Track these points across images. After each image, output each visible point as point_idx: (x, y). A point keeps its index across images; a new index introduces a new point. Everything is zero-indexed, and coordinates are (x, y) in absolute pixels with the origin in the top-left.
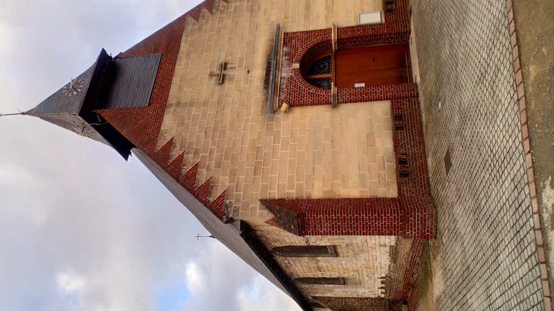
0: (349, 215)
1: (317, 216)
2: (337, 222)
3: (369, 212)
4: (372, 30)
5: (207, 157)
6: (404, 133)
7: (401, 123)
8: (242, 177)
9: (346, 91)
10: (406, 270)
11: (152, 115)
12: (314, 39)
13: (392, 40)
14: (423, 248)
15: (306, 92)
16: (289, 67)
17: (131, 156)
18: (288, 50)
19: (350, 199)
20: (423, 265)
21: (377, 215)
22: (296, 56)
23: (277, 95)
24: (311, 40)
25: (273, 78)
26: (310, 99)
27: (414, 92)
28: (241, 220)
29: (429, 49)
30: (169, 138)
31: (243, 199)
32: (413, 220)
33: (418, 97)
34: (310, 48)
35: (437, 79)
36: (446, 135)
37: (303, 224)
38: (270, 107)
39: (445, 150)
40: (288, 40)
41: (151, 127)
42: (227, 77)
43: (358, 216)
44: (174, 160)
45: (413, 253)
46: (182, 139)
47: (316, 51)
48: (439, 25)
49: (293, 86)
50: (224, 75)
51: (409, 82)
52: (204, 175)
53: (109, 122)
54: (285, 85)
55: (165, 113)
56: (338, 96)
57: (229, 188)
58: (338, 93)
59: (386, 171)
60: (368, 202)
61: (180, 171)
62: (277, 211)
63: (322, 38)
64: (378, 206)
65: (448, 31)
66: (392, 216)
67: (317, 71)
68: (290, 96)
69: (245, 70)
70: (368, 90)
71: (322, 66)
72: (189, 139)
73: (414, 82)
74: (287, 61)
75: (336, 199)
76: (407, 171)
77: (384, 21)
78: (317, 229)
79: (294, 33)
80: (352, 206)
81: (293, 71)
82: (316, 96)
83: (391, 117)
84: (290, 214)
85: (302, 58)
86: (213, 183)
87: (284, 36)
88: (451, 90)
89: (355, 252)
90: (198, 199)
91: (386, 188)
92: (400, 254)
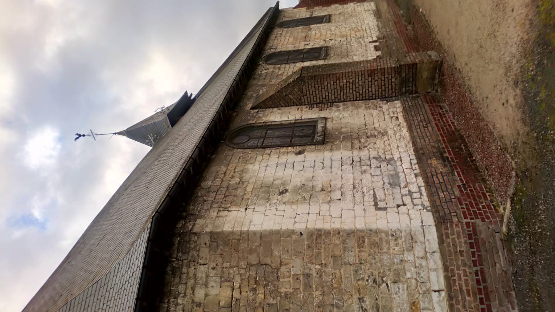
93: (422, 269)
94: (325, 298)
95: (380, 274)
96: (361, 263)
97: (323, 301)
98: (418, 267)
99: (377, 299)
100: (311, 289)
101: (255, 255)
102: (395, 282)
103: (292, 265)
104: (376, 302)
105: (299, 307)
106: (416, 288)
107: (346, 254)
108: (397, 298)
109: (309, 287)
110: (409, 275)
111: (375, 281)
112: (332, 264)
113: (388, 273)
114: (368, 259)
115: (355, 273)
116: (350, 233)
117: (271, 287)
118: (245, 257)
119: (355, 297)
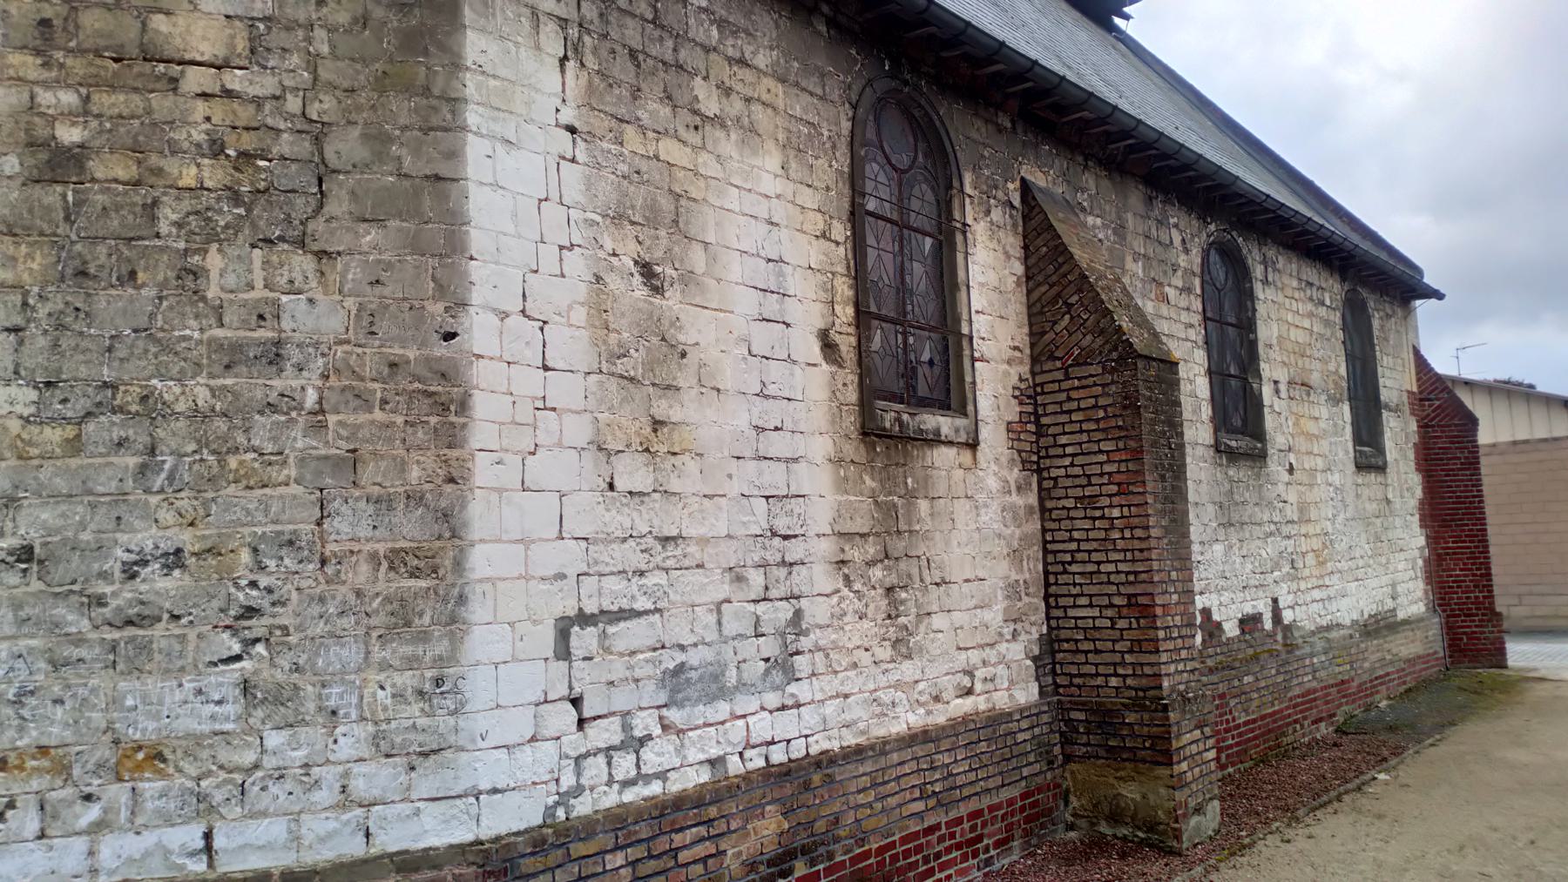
10: (1343, 682)
93: (298, 790)
94: (182, 424)
95: (278, 633)
96: (323, 562)
97: (172, 414)
98: (308, 774)
99: (177, 618)
100: (217, 369)
101: (361, 153)
102: (246, 687)
103: (319, 296)
104: (166, 616)
105: (143, 322)
106: (221, 767)
107: (362, 504)
108: (178, 696)
109: (226, 360)
110: (274, 739)
111: (251, 612)
112: (323, 452)
113: (285, 662)
114: (343, 589)
115: (287, 537)
116: (450, 524)
117: (227, 214)
118: (353, 117)
119: (187, 539)
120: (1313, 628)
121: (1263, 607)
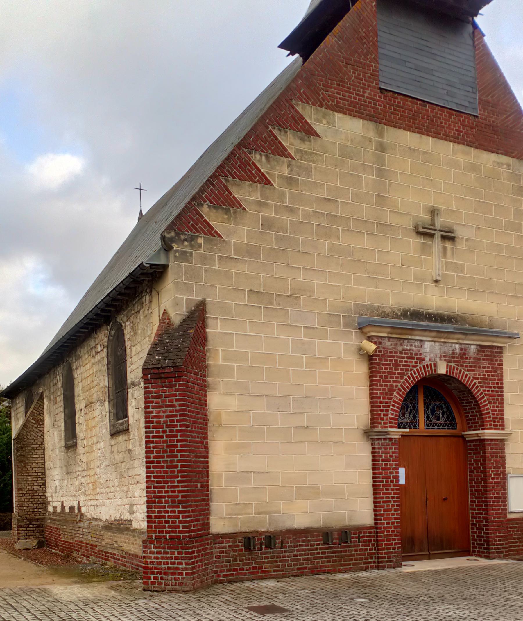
0: (179, 454)
1: (177, 400)
2: (168, 434)
3: (185, 486)
4: (495, 497)
5: (283, 202)
6: (318, 544)
7: (334, 541)
8: (245, 268)
9: (393, 452)
11: (363, 96)
12: (488, 399)
13: (477, 529)
14: (129, 572)
15: (394, 384)
16: (441, 356)
17: (288, 55)
18: (471, 354)
19: (207, 457)
20: (101, 571)
21: (180, 498)
22: (459, 368)
23: (391, 334)
24: (486, 395)
25: (422, 326)
26: (381, 391)
27: (387, 562)
28: (168, 266)
29: (457, 586)
30: (318, 128)
31: (206, 270)
32: (173, 556)
33: (378, 568)
34: (472, 393)
35: (406, 598)
36: (312, 607)
37: (163, 376)
38: (373, 321)
39: (288, 606)
40: (490, 354)
41: (338, 93)
42: (428, 242)
43: (179, 469)
44: (277, 139)
45: (121, 556)
46: (316, 154)
47: (466, 403)
48: (496, 603)
49: (406, 362)
50: (432, 235)
51: (403, 555)
52: (250, 196)
53: (352, 9)
54: (408, 348)
55: (366, 122)
56: (385, 439)
57: (225, 245)
58: (391, 439)
59: (254, 515)
60: (202, 486)
61: (257, 151)
62: (185, 331)
63: (489, 413)
64: (195, 501)
65: (484, 615)
66: (179, 523)
67: (430, 404)
68: (388, 356)
69: (439, 275)
70: (392, 490)
71: (439, 413)
72: (315, 169)
73: (403, 563)
74: (451, 352)
75: (206, 433)
76: (254, 548)
77: (509, 516)
78: (155, 400)
79: (502, 365)
80: (194, 459)
81: (432, 363)
82: (386, 403)
83: (346, 526)
84: (181, 353)
85: (455, 378)
86: (235, 213)
87: (498, 347)
88: (386, 617)
89: (119, 464)
90: (206, 183)
91: (226, 515)
92: (119, 535)
120: (90, 517)
121: (75, 504)
